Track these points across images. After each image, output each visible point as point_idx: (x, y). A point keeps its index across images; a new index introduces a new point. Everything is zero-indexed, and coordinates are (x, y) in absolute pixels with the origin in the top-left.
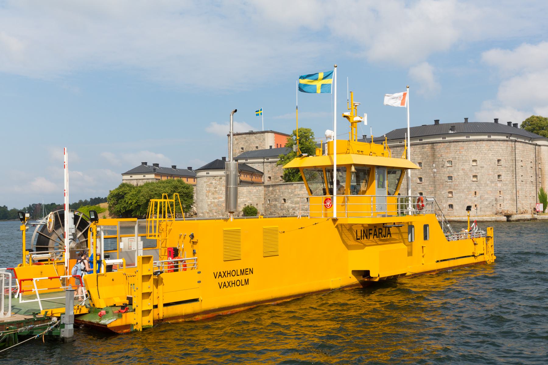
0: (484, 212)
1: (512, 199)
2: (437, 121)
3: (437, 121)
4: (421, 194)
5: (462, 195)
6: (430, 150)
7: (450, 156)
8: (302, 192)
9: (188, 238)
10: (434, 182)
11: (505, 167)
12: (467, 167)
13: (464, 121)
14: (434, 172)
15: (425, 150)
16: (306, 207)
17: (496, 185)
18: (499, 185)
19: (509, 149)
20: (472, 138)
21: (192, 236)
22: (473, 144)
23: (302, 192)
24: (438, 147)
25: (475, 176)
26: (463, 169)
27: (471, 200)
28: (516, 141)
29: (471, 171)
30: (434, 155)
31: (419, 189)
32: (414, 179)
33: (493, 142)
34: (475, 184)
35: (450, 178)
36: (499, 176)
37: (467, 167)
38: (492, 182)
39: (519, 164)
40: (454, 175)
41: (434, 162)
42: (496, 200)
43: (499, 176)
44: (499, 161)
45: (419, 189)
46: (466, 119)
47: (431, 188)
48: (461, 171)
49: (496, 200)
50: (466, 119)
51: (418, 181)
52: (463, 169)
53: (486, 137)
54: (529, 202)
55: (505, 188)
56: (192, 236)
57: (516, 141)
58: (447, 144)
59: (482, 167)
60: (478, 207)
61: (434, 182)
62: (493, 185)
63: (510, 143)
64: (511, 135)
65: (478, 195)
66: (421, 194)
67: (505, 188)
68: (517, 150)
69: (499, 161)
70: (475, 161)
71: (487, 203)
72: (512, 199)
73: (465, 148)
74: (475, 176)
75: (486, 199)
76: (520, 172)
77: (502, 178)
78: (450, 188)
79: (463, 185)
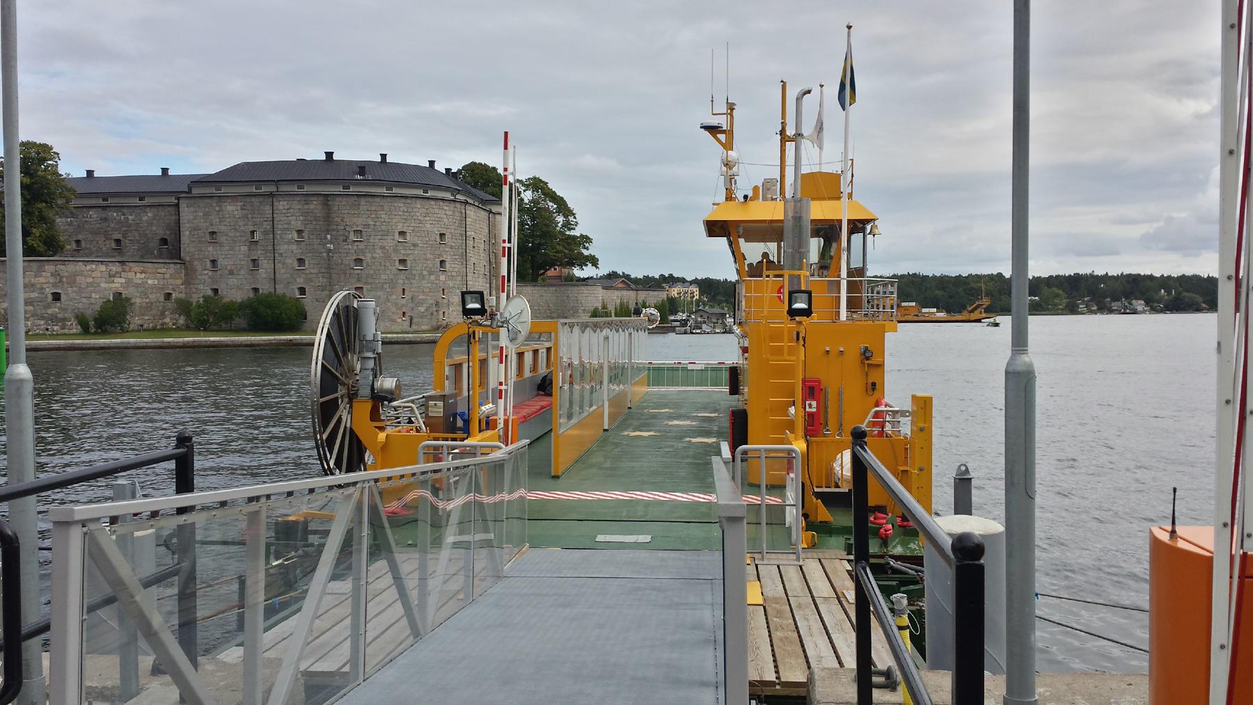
0: (418, 324)
2: (329, 155)
3: (329, 155)
4: (302, 291)
5: (379, 293)
6: (320, 207)
7: (359, 222)
8: (42, 280)
9: (853, 356)
10: (329, 268)
11: (452, 247)
12: (389, 243)
13: (379, 159)
14: (330, 250)
15: (312, 207)
16: (50, 311)
17: (437, 278)
18: (442, 278)
20: (395, 191)
21: (866, 355)
22: (400, 204)
23: (42, 280)
24: (336, 204)
25: (402, 262)
26: (381, 248)
27: (396, 304)
28: (467, 203)
29: (396, 251)
30: (328, 218)
31: (299, 280)
32: (289, 261)
33: (433, 202)
34: (402, 276)
35: (359, 261)
36: (442, 262)
38: (431, 273)
39: (470, 243)
40: (367, 258)
41: (328, 231)
42: (437, 304)
43: (442, 262)
44: (442, 235)
45: (300, 280)
46: (384, 156)
47: (322, 280)
48: (379, 251)
49: (437, 304)
50: (384, 156)
51: (296, 264)
52: (382, 248)
53: (420, 192)
55: (451, 284)
56: (866, 355)
58: (353, 199)
59: (415, 245)
61: (329, 268)
62: (432, 277)
63: (458, 205)
64: (459, 192)
65: (408, 295)
66: (302, 291)
67: (451, 284)
69: (442, 235)
70: (402, 233)
71: (422, 309)
73: (386, 208)
74: (402, 262)
75: (420, 303)
76: (472, 259)
77: (448, 265)
78: (359, 280)
79: (383, 277)
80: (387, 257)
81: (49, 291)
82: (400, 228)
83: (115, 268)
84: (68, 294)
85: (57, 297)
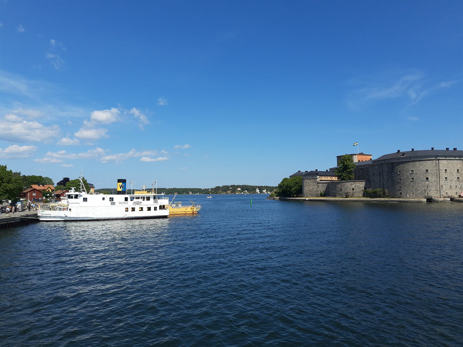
1: (436, 190)
12: (408, 174)
18: (427, 183)
19: (434, 164)
28: (439, 160)
35: (400, 179)
36: (427, 179)
37: (408, 174)
38: (422, 181)
40: (402, 178)
42: (425, 190)
54: (455, 191)
57: (439, 160)
60: (415, 194)
64: (437, 156)
68: (440, 165)
69: (427, 171)
72: (436, 190)
77: (429, 179)
80: (408, 178)
81: (340, 188)
82: (412, 169)
83: (352, 183)
84: (343, 188)
85: (341, 189)
